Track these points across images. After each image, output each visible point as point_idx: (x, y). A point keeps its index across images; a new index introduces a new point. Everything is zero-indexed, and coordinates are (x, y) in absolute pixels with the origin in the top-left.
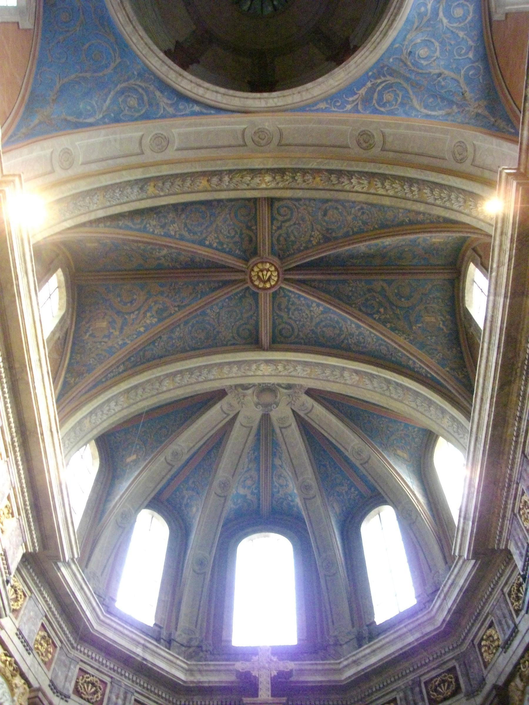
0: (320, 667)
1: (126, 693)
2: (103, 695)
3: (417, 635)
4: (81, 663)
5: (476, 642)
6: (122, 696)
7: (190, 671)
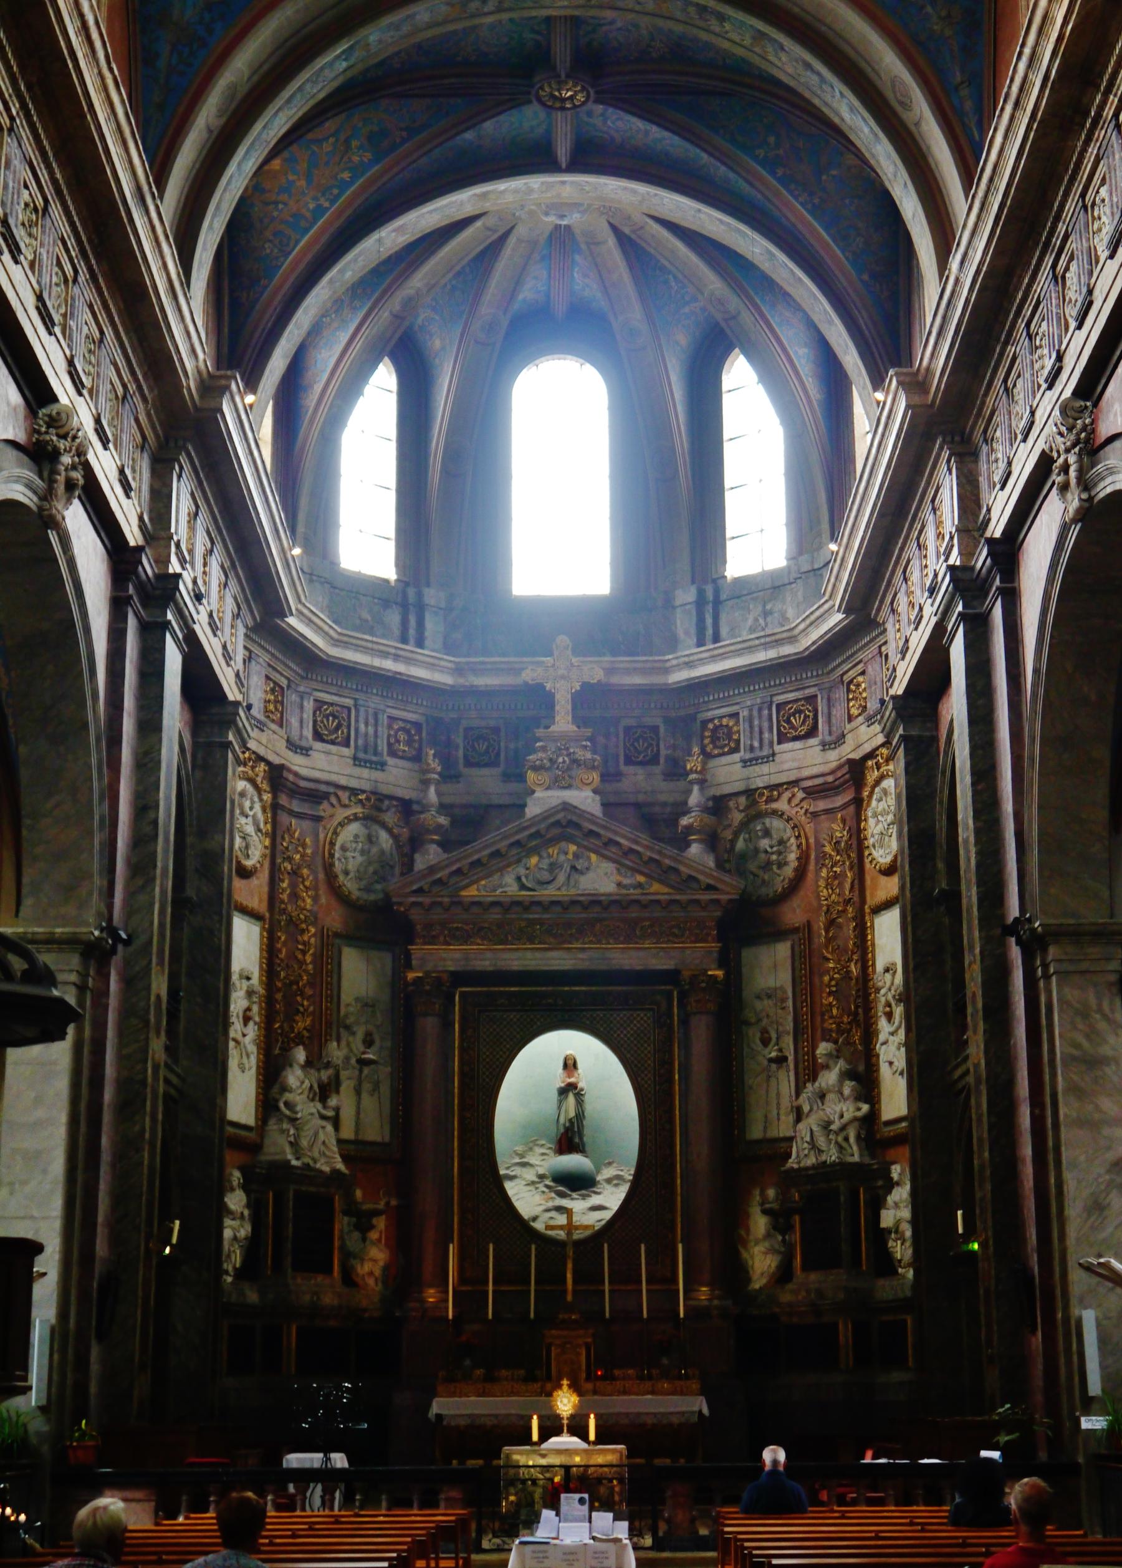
0: (639, 665)
1: (376, 715)
2: (349, 727)
3: (772, 654)
5: (846, 678)
6: (371, 720)
7: (459, 670)
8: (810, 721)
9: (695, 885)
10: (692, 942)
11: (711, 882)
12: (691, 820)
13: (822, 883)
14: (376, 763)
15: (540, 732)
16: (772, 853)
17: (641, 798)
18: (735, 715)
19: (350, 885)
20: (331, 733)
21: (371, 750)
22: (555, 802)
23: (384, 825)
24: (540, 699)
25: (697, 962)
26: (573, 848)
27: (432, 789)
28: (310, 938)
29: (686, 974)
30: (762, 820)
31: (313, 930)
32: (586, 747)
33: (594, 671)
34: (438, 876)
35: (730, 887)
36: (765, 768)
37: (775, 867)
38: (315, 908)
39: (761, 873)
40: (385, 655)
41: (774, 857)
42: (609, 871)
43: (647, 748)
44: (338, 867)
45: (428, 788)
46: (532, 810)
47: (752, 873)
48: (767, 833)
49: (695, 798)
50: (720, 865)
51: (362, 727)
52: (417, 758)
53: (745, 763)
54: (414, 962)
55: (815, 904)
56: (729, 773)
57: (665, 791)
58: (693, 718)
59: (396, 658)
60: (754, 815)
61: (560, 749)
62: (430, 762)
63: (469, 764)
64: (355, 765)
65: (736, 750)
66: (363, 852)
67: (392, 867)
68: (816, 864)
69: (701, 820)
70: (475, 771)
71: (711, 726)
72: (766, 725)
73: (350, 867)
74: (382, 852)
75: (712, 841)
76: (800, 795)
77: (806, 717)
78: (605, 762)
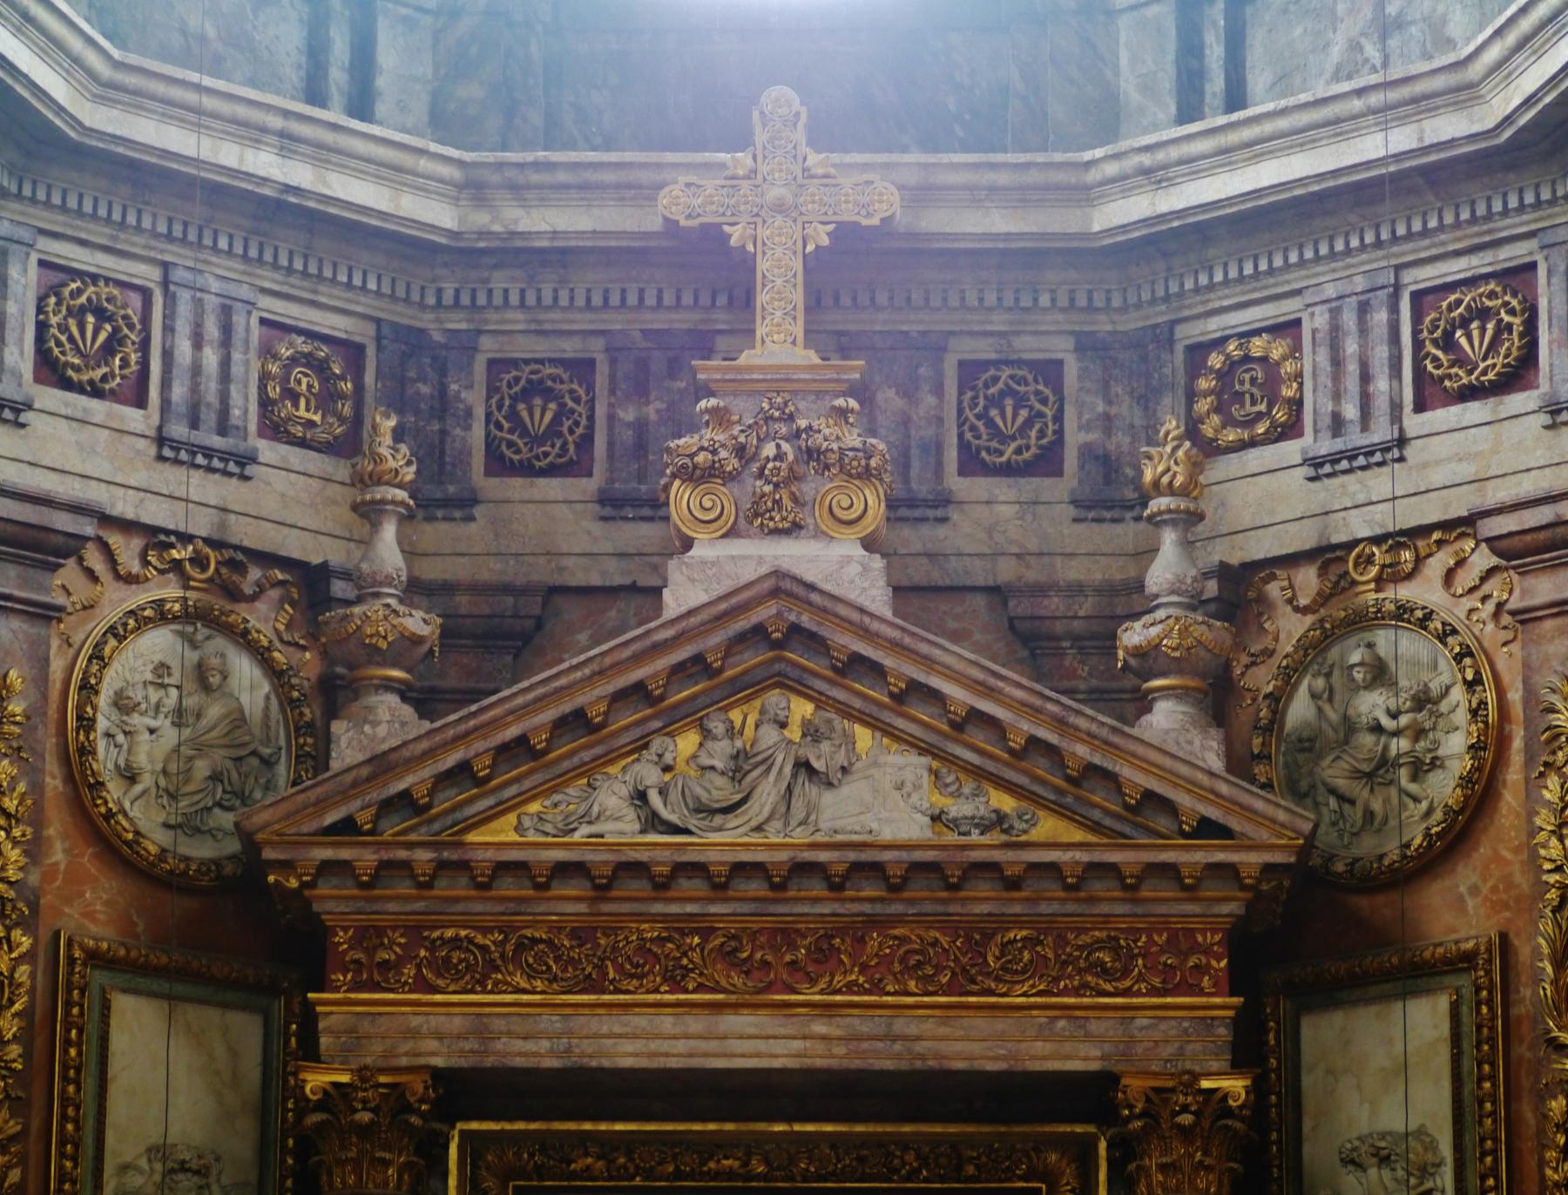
0: (1003, 178)
1: (226, 312)
3: (1402, 139)
4: (44, 243)
6: (212, 329)
7: (473, 189)
8: (1513, 344)
9: (1163, 823)
10: (1153, 992)
11: (1213, 813)
12: (1154, 631)
13: (1545, 820)
14: (226, 456)
15: (708, 369)
16: (1397, 733)
17: (1006, 571)
18: (1289, 328)
19: (144, 819)
20: (90, 361)
21: (209, 418)
22: (750, 573)
23: (243, 638)
24: (714, 272)
25: (1168, 1051)
26: (802, 709)
27: (389, 531)
28: (17, 962)
29: (1135, 1085)
30: (1368, 636)
31: (25, 942)
32: (843, 413)
33: (872, 191)
34: (401, 786)
35: (1268, 831)
36: (1379, 483)
37: (1404, 774)
38: (34, 878)
39: (1359, 791)
40: (253, 134)
41: (1404, 744)
42: (909, 776)
43: (1028, 423)
44: (105, 758)
45: (375, 526)
46: (684, 593)
47: (1333, 791)
48: (1380, 674)
49: (1166, 568)
50: (1239, 764)
51: (184, 348)
52: (349, 445)
53: (1319, 467)
54: (324, 1041)
55: (1522, 881)
56: (1270, 498)
57: (1080, 551)
58: (1164, 336)
59: (288, 143)
60: (1341, 622)
61: (769, 419)
62: (384, 451)
63: (498, 464)
64: (161, 458)
65: (1291, 429)
66: (180, 717)
67: (268, 763)
68: (1530, 760)
69: (1185, 631)
70: (516, 486)
71: (1216, 360)
72: (1381, 353)
73: (141, 760)
74: (238, 719)
75: (1217, 696)
76: (1483, 559)
77: (1503, 329)
78: (903, 464)
